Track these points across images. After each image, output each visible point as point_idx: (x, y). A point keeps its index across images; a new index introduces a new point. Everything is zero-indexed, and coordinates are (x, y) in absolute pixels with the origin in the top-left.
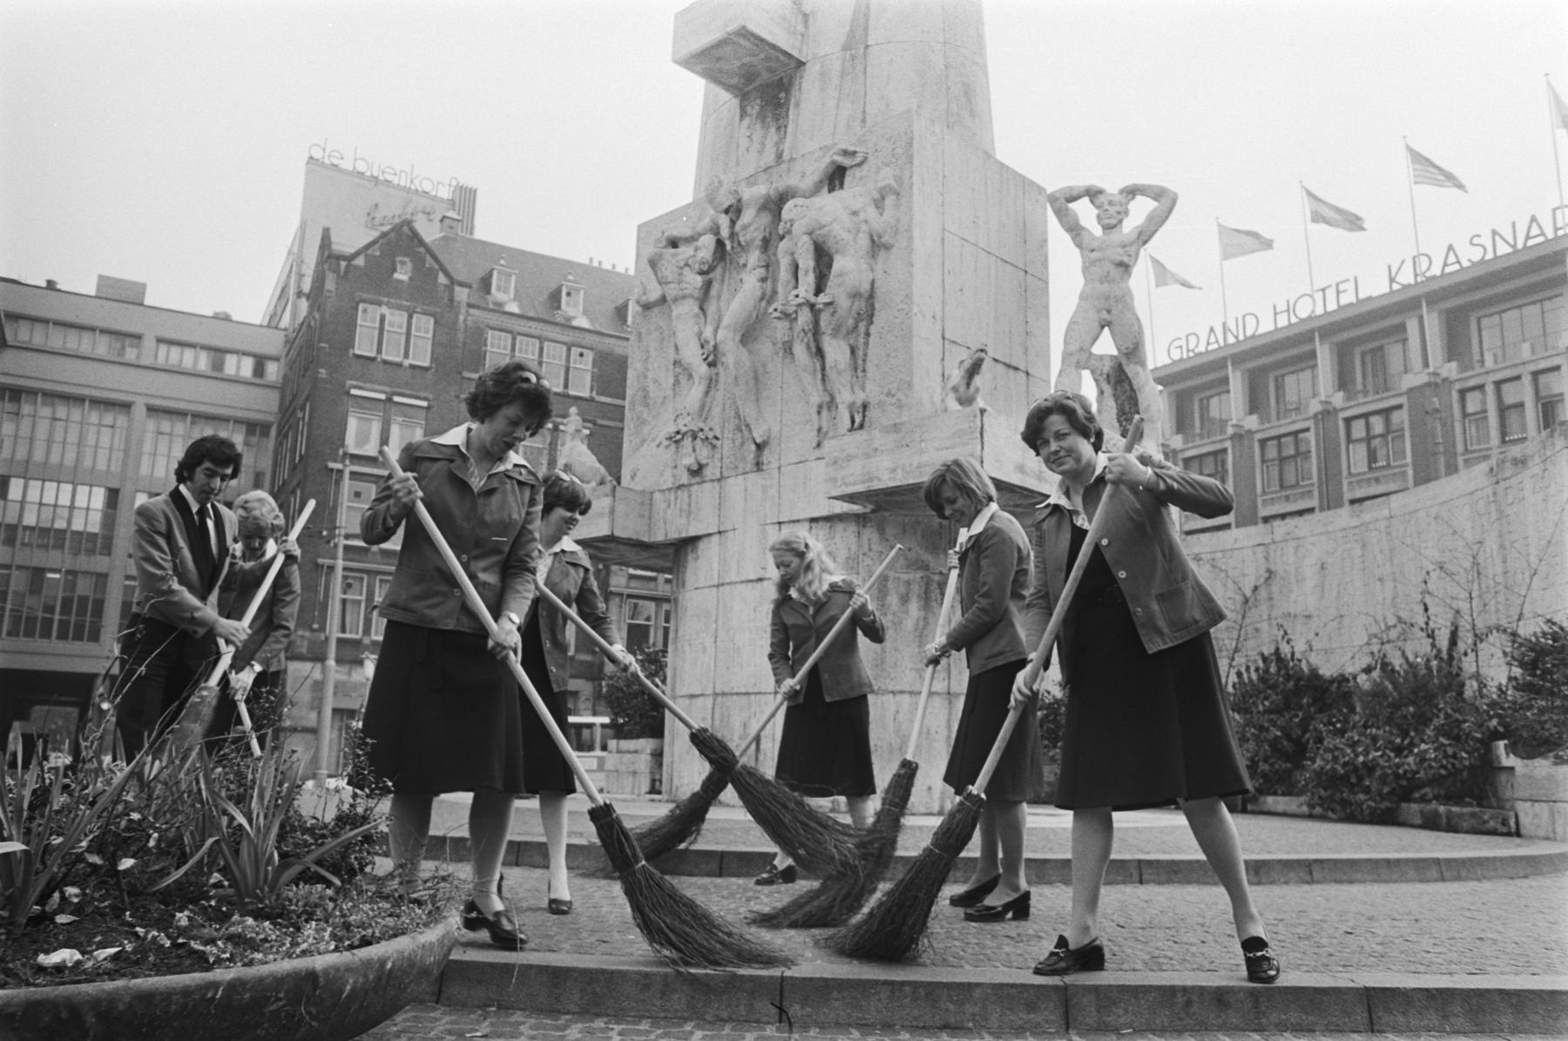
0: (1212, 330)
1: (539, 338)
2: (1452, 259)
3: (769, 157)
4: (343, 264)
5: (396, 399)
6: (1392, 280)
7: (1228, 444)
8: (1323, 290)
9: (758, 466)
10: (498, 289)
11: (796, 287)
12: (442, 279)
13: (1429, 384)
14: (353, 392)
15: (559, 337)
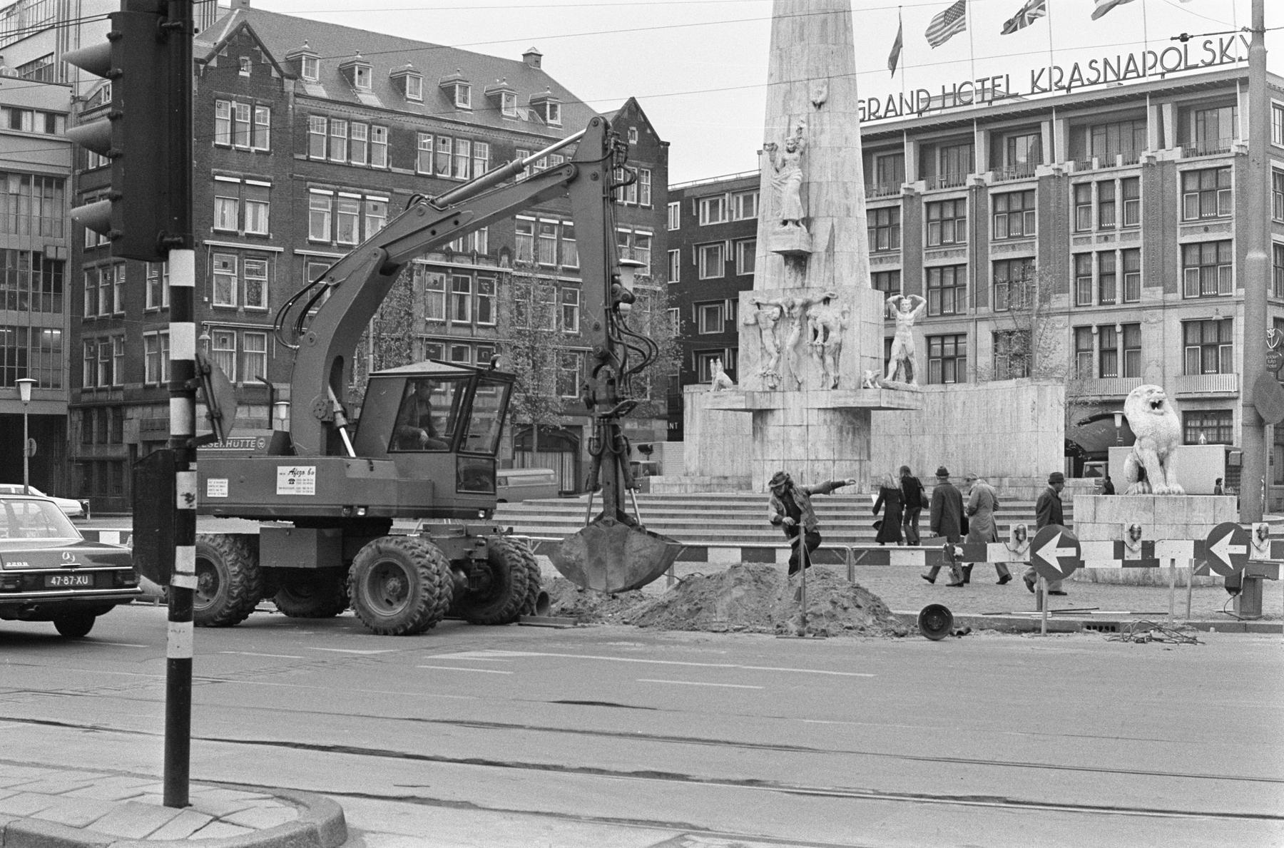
0: (891, 99)
1: (350, 121)
2: (1077, 76)
3: (799, 284)
4: (202, 66)
5: (248, 182)
6: (1034, 83)
7: (900, 203)
8: (983, 81)
9: (799, 390)
10: (307, 73)
11: (816, 337)
12: (275, 74)
13: (1054, 176)
14: (217, 178)
15: (365, 118)
